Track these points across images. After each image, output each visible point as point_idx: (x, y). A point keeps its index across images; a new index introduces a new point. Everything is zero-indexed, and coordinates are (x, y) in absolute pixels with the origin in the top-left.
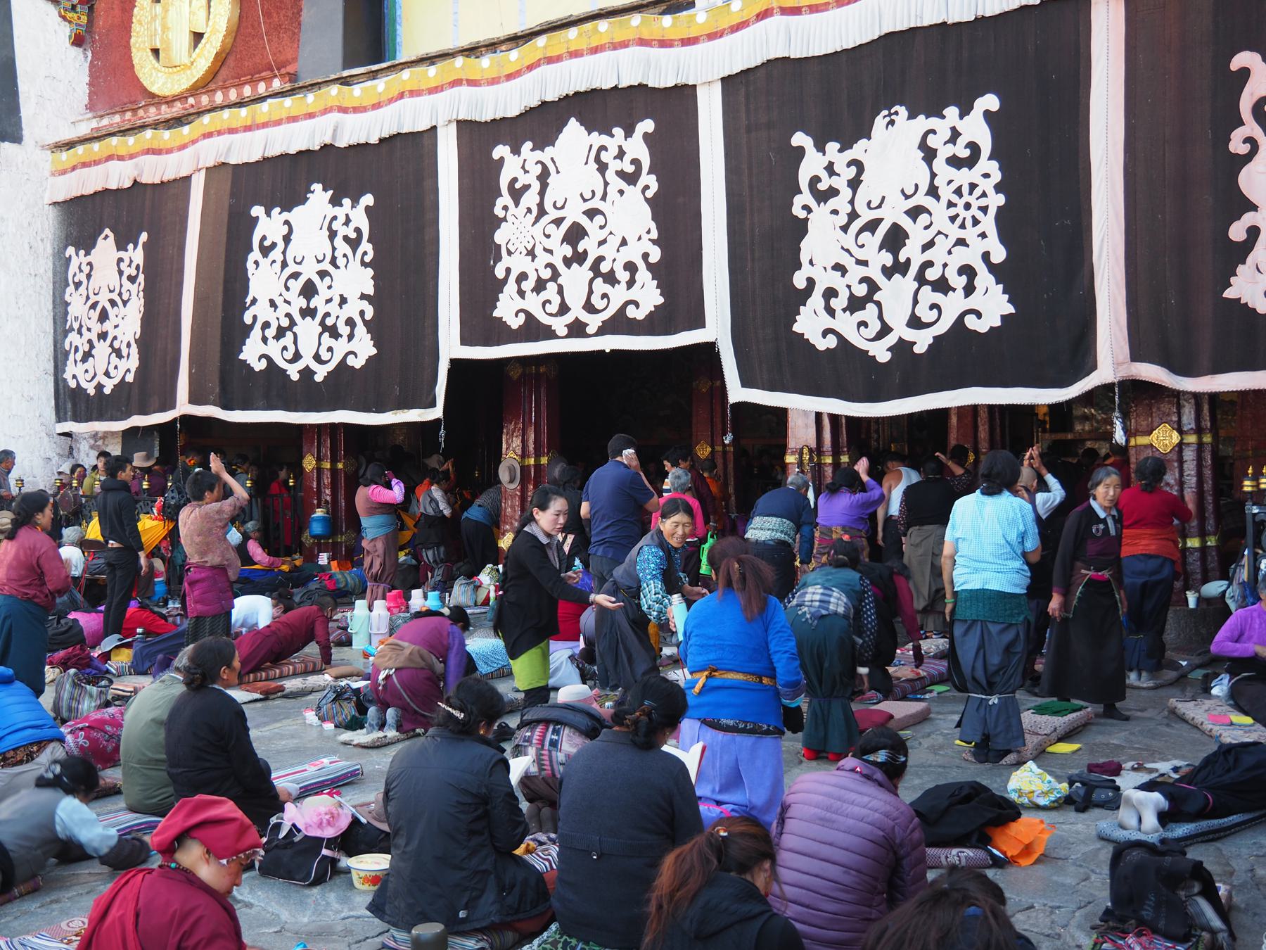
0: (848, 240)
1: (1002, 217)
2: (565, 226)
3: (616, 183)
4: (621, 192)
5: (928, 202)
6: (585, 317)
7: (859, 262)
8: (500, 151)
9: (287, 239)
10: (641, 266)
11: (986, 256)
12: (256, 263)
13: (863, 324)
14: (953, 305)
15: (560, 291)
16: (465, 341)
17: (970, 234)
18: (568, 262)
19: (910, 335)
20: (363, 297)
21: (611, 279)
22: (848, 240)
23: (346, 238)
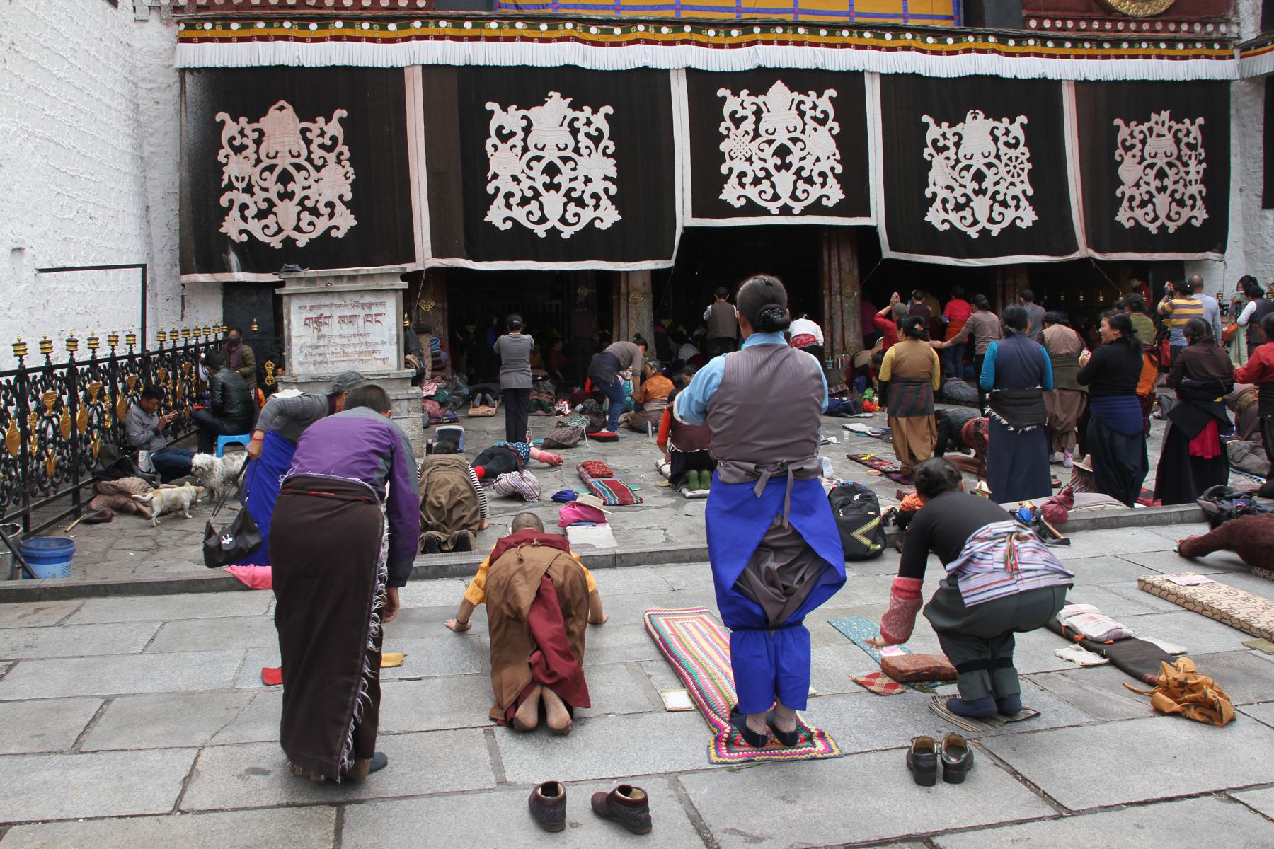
0: (956, 174)
1: (1031, 174)
2: (774, 146)
3: (811, 124)
4: (815, 130)
5: (996, 162)
6: (791, 203)
7: (961, 186)
8: (721, 92)
9: (527, 130)
10: (830, 174)
11: (1024, 192)
13: (963, 218)
14: (1010, 214)
15: (773, 185)
16: (696, 214)
17: (1017, 180)
18: (778, 168)
19: (989, 226)
20: (606, 178)
22: (956, 174)
23: (588, 135)
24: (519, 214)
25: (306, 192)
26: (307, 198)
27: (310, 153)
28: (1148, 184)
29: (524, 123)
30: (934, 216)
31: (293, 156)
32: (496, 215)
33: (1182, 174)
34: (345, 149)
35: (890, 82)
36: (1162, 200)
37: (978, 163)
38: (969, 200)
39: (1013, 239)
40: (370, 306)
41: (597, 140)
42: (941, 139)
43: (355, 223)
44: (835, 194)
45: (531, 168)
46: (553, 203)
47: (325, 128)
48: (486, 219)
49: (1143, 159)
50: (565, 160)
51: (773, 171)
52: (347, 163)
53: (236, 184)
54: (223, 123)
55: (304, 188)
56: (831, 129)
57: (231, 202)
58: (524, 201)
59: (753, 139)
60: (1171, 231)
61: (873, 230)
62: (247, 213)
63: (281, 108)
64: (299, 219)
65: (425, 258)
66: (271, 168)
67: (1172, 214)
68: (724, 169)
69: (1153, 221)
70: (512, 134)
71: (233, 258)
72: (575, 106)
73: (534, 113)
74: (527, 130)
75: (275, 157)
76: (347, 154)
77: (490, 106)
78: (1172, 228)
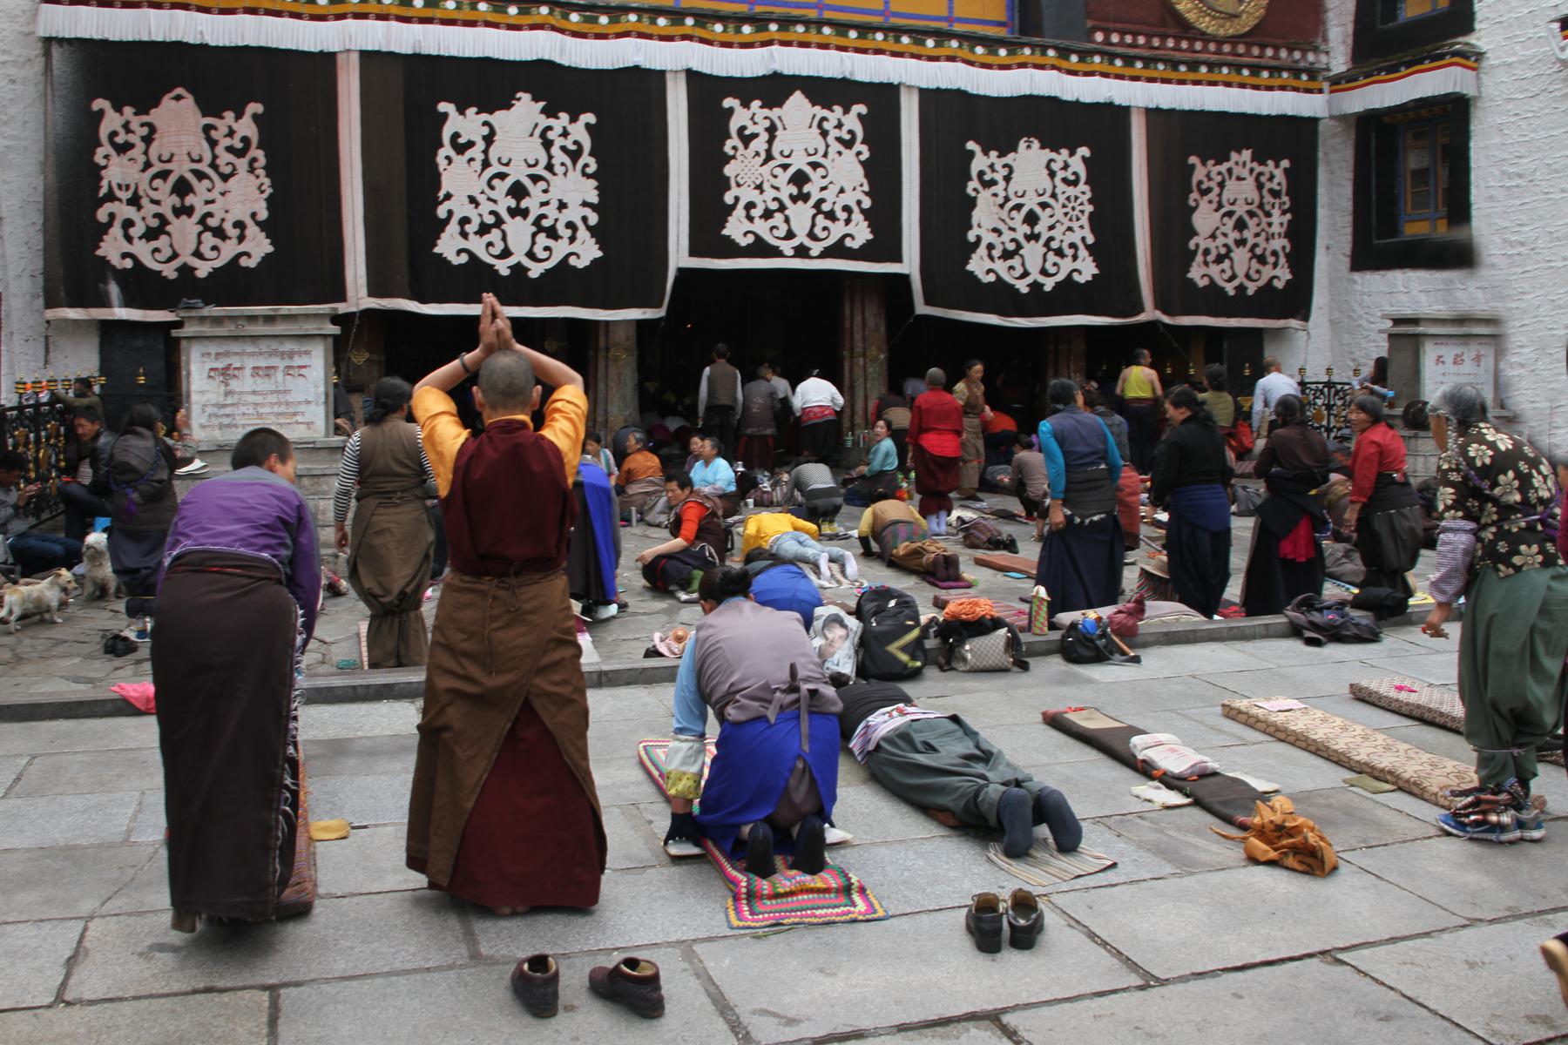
0: (1004, 214)
1: (1092, 217)
2: (791, 171)
3: (835, 146)
4: (840, 153)
5: (1051, 201)
6: (808, 242)
8: (728, 103)
9: (489, 139)
10: (856, 209)
12: (448, 158)
13: (1011, 268)
14: (1066, 265)
15: (787, 220)
17: (1075, 225)
18: (794, 199)
19: (1041, 279)
20: (585, 204)
21: (831, 215)
22: (1004, 214)
23: (563, 149)
24: (477, 245)
25: (209, 208)
26: (210, 215)
27: (215, 157)
28: (1225, 235)
29: (486, 130)
30: (978, 265)
31: (193, 161)
32: (448, 246)
33: (1264, 225)
34: (260, 154)
35: (931, 99)
36: (1241, 256)
37: (1031, 203)
38: (1019, 246)
39: (1069, 295)
40: (291, 355)
41: (575, 155)
42: (988, 171)
43: (270, 249)
44: (861, 233)
45: (492, 188)
46: (519, 233)
47: (235, 126)
48: (436, 250)
49: (1220, 206)
50: (535, 179)
51: (787, 202)
52: (262, 172)
53: (118, 193)
54: (101, 113)
55: (207, 202)
56: (859, 153)
57: (112, 216)
58: (484, 229)
59: (765, 162)
60: (1250, 292)
61: (904, 279)
62: (132, 231)
63: (178, 98)
64: (200, 243)
65: (358, 297)
66: (164, 175)
67: (1252, 273)
68: (728, 198)
69: (1230, 280)
70: (471, 144)
71: (114, 290)
72: (550, 112)
73: (498, 118)
74: (489, 139)
75: (169, 161)
76: (262, 161)
77: (443, 107)
78: (1251, 289)
